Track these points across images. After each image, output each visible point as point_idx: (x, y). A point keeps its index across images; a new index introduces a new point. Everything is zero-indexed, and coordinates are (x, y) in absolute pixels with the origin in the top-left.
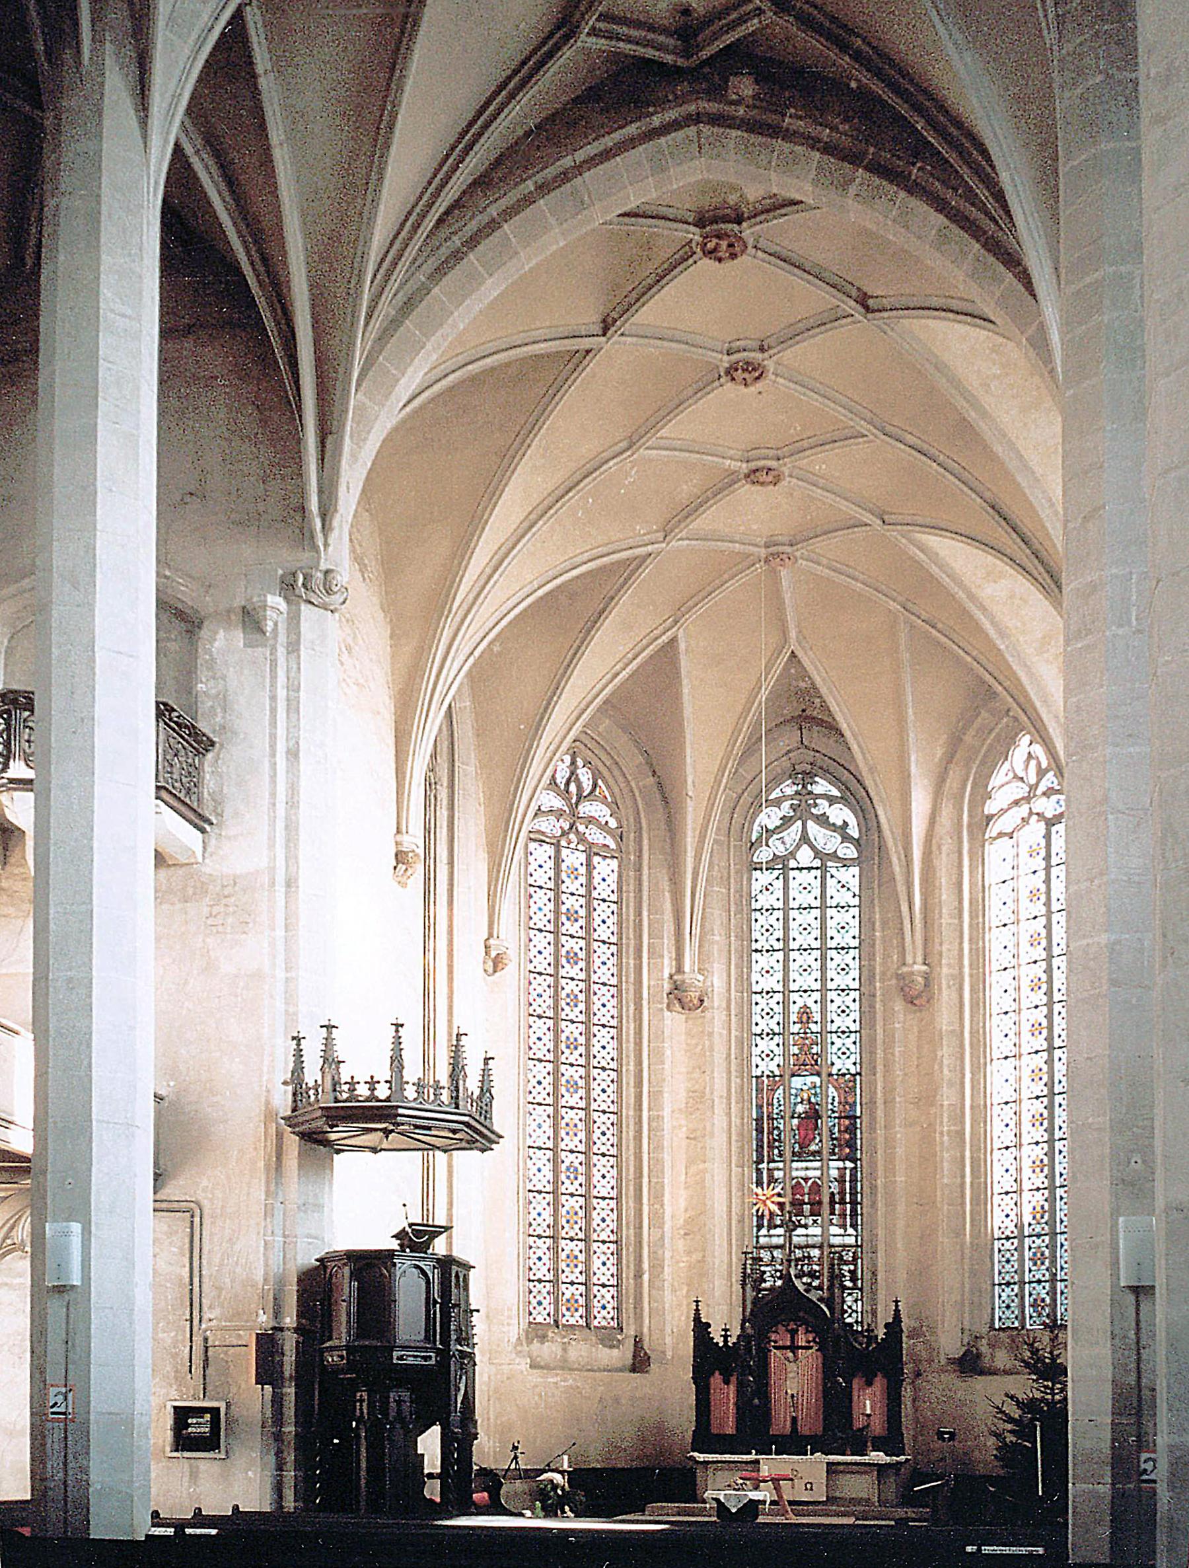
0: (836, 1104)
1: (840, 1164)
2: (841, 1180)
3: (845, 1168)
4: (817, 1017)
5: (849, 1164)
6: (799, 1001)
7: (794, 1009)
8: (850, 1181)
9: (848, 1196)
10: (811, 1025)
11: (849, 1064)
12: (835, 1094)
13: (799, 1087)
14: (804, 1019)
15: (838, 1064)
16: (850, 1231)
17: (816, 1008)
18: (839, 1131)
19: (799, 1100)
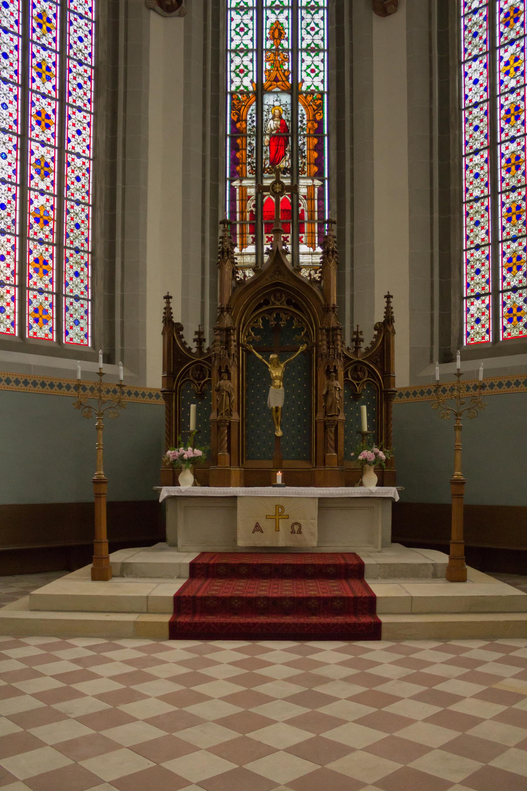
0: (305, 122)
1: (309, 182)
2: (309, 198)
3: (314, 186)
4: (288, 33)
5: (317, 183)
6: (270, 18)
7: (267, 24)
8: (319, 200)
9: (316, 213)
10: (283, 42)
11: (317, 82)
12: (304, 112)
13: (271, 103)
14: (276, 35)
15: (308, 81)
16: (319, 250)
17: (287, 25)
18: (309, 149)
19: (271, 116)
